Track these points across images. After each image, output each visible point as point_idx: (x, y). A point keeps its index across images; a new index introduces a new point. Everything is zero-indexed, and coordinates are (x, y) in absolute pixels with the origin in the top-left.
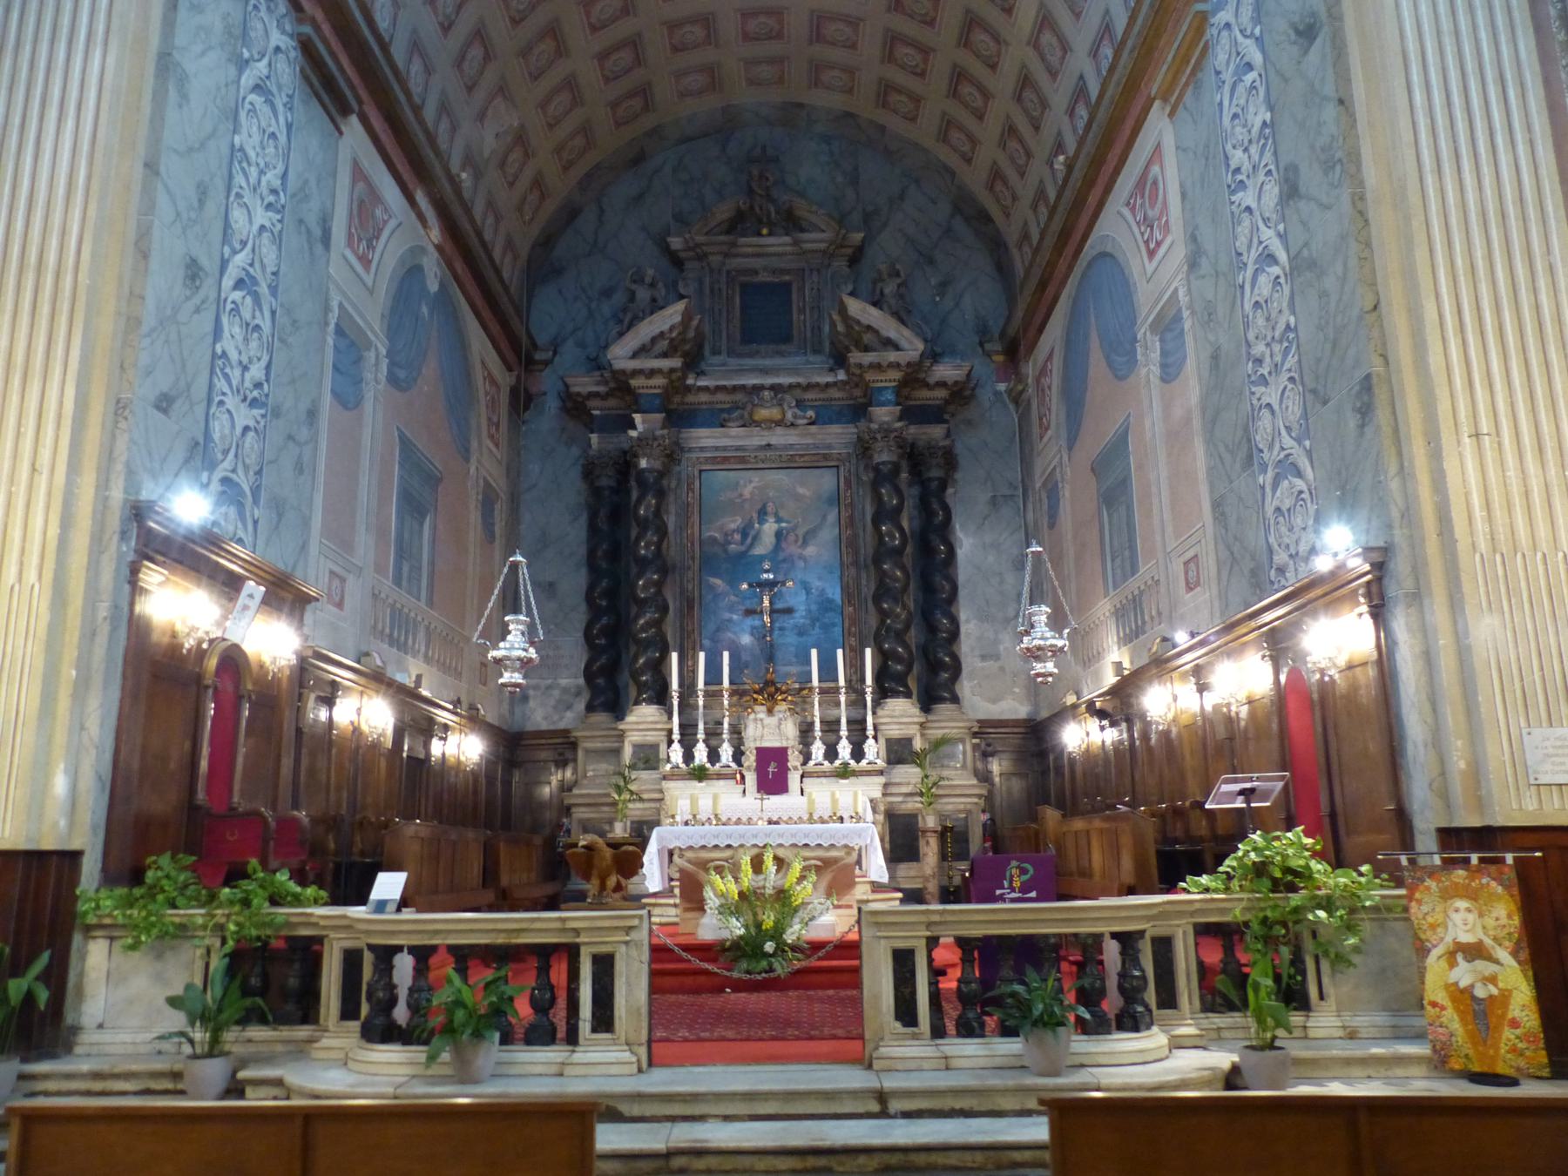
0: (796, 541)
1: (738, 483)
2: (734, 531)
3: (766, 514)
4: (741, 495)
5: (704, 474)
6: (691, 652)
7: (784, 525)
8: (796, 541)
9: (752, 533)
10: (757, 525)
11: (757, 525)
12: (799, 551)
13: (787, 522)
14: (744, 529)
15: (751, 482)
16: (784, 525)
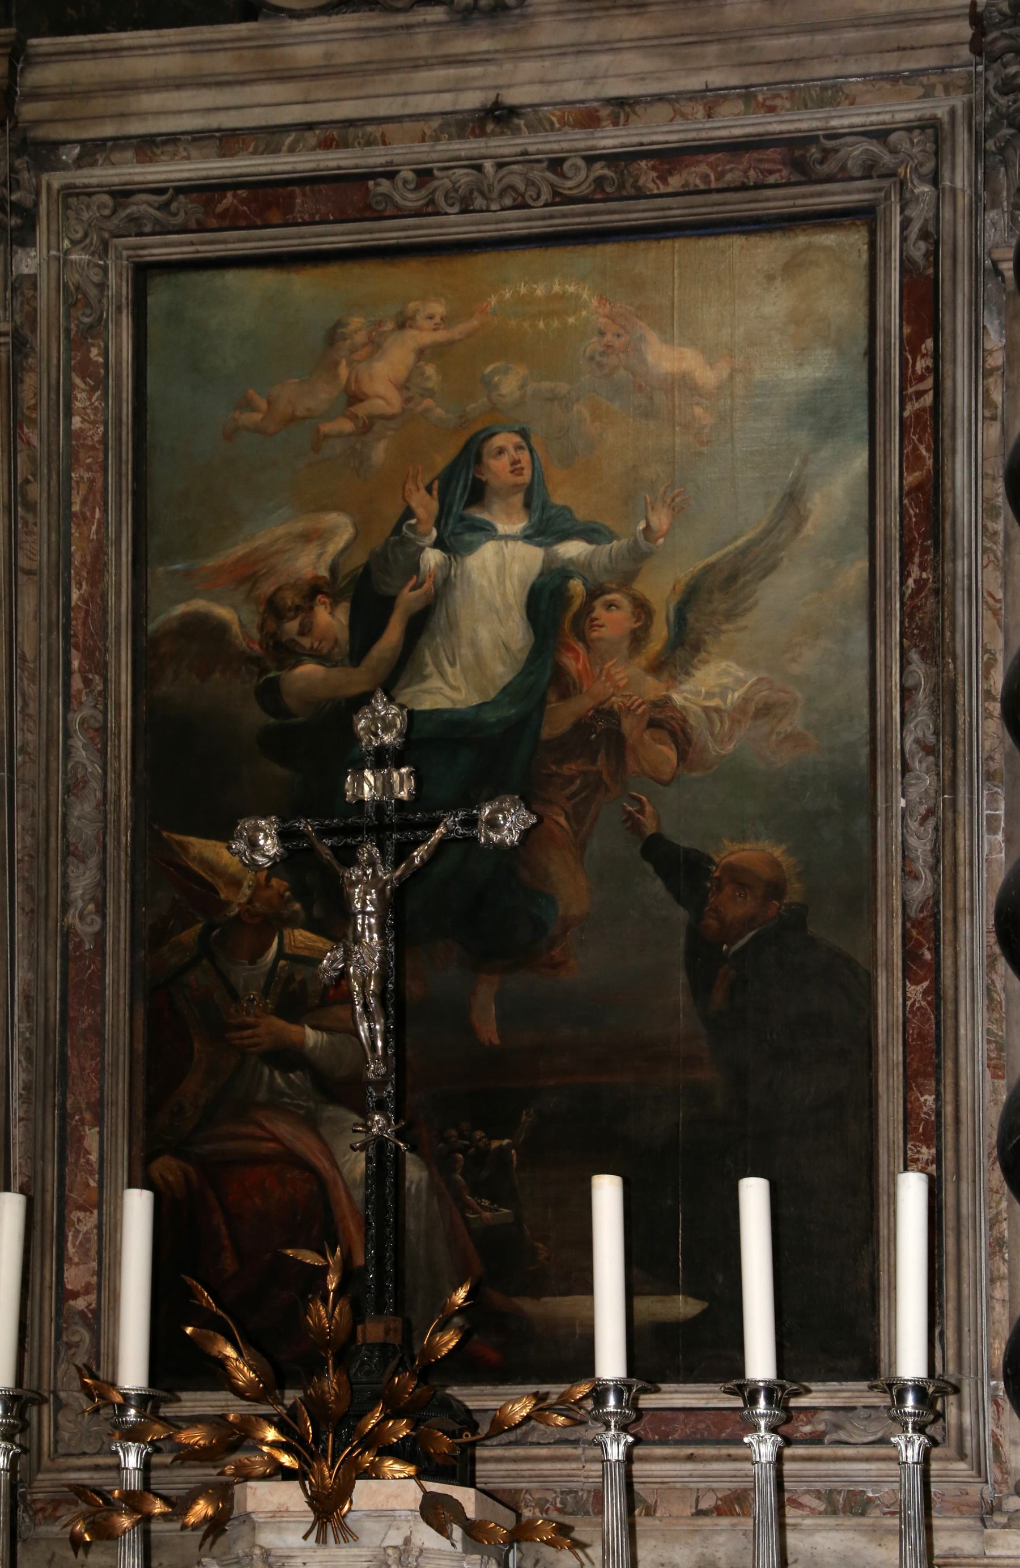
0: (638, 638)
1: (333, 336)
2: (314, 590)
3: (478, 494)
4: (354, 397)
5: (159, 297)
6: (85, 1222)
7: (573, 549)
8: (638, 638)
9: (409, 599)
10: (432, 558)
11: (432, 558)
12: (652, 687)
13: (590, 533)
14: (365, 577)
15: (404, 323)
16: (573, 549)
